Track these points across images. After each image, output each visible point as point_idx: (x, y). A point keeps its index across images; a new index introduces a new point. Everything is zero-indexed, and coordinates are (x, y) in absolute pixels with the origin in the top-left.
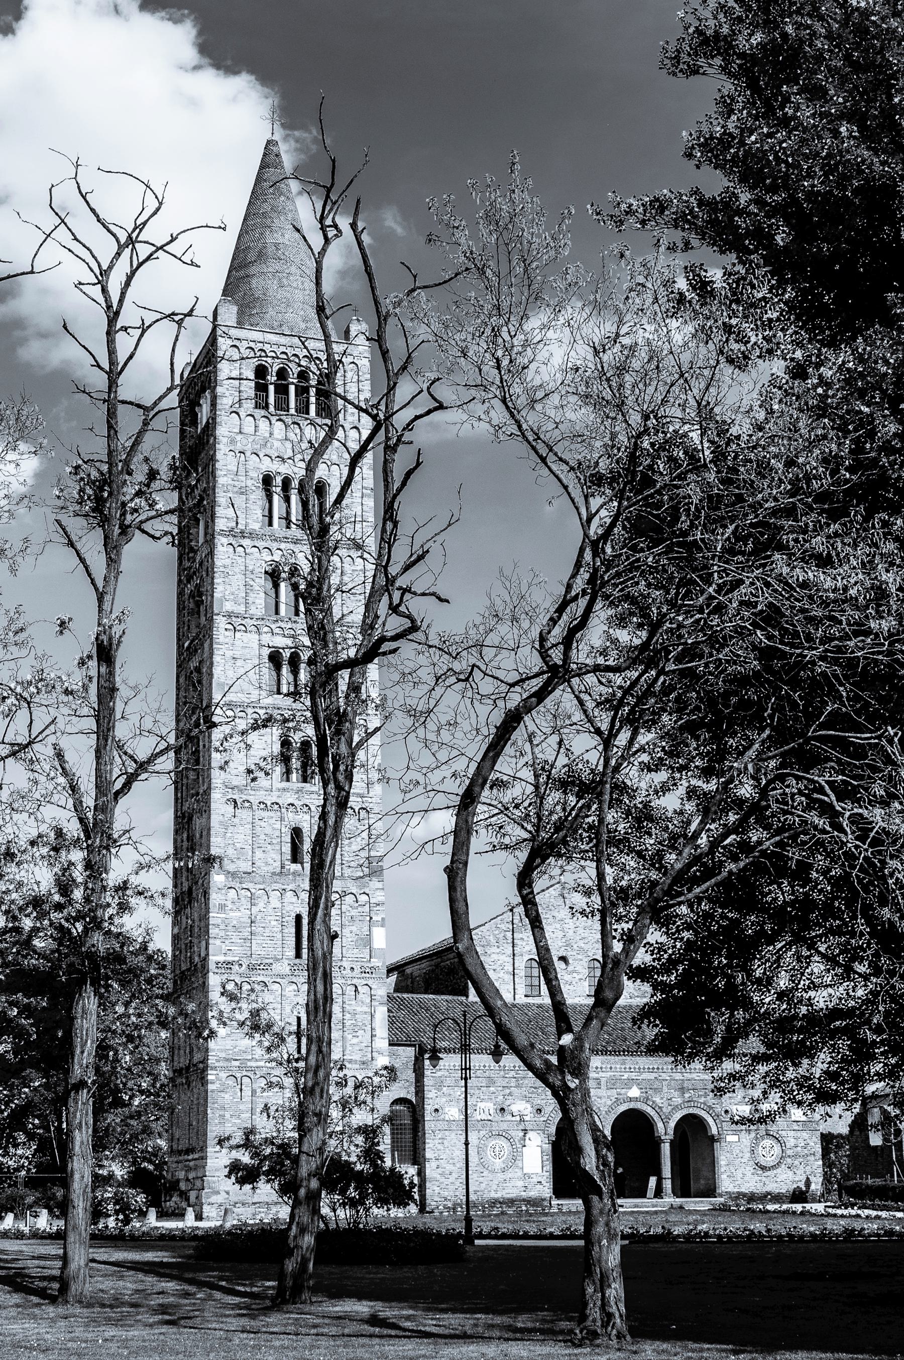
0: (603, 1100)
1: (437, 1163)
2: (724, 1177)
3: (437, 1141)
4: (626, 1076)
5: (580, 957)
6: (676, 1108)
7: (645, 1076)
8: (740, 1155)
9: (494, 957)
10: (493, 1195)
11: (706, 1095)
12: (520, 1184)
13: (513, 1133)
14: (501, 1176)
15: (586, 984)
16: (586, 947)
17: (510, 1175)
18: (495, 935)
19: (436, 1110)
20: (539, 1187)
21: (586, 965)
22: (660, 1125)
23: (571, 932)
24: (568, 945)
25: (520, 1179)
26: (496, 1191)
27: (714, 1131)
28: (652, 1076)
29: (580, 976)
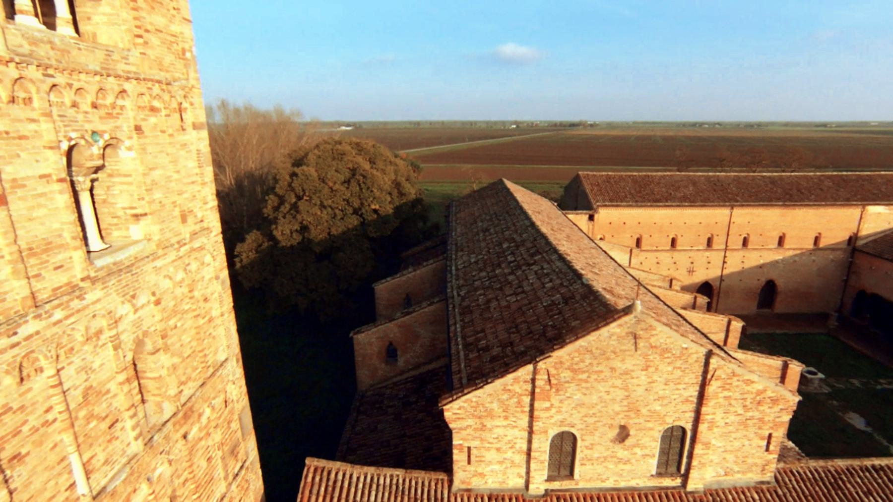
9: (500, 431)
18: (501, 402)
23: (640, 391)
24: (633, 409)
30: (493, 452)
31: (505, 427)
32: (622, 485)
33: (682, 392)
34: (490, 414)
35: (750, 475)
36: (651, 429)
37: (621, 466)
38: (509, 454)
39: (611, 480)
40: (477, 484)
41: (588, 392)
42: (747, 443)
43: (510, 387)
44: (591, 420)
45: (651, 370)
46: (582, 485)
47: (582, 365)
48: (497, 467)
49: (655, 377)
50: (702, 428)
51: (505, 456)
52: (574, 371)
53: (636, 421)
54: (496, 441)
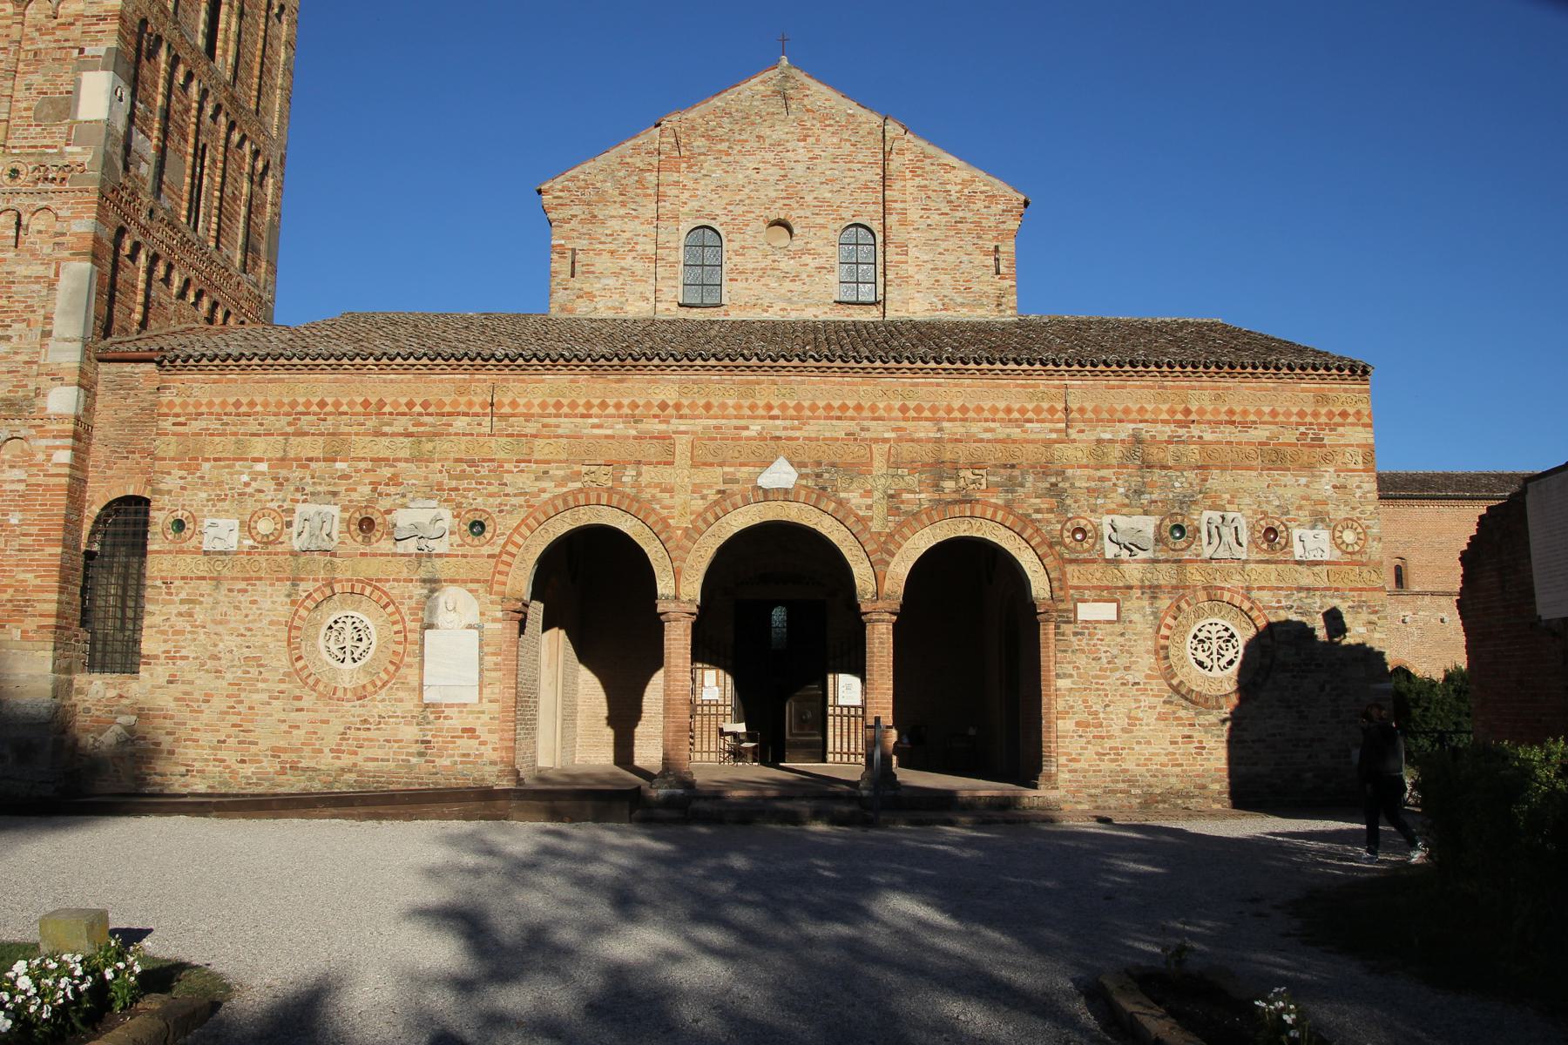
0: (678, 499)
1: (171, 669)
2: (1065, 725)
3: (174, 609)
4: (755, 428)
5: (820, 220)
6: (914, 519)
7: (811, 429)
8: (1122, 661)
9: (614, 224)
10: (327, 761)
11: (1011, 486)
12: (411, 732)
13: (396, 590)
14: (353, 710)
15: (833, 279)
16: (836, 200)
17: (381, 708)
19: (179, 525)
20: (466, 744)
21: (834, 237)
22: (862, 573)
23: (800, 168)
25: (408, 719)
26: (337, 752)
27: (1039, 587)
28: (840, 429)
29: (820, 262)
30: (606, 256)
31: (622, 217)
32: (793, 316)
33: (857, 174)
34: (602, 198)
35: (980, 312)
36: (824, 227)
37: (788, 284)
38: (628, 262)
39: (776, 308)
40: (582, 309)
41: (730, 169)
42: (965, 258)
43: (628, 160)
44: (739, 210)
45: (811, 140)
46: (735, 315)
47: (720, 131)
48: (611, 282)
49: (817, 152)
50: (892, 220)
51: (623, 263)
52: (709, 138)
53: (802, 213)
54: (609, 239)
